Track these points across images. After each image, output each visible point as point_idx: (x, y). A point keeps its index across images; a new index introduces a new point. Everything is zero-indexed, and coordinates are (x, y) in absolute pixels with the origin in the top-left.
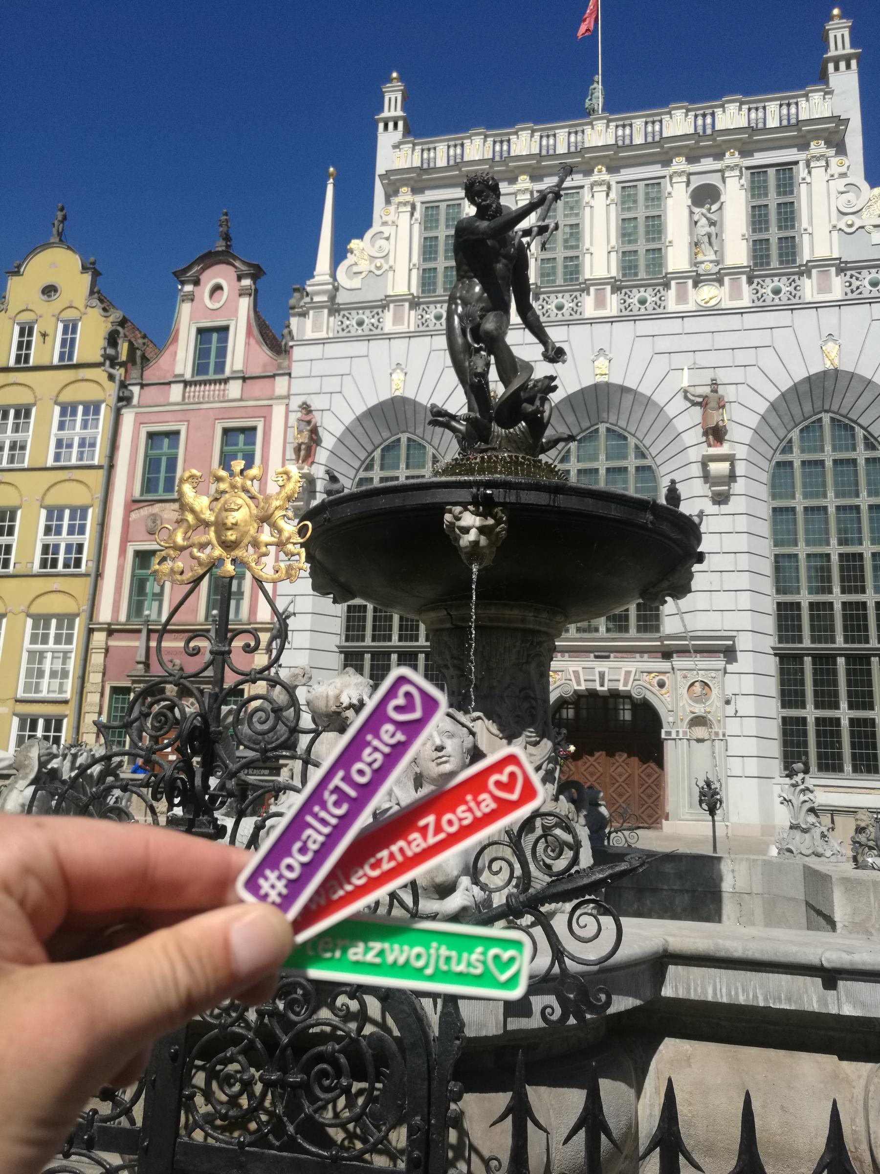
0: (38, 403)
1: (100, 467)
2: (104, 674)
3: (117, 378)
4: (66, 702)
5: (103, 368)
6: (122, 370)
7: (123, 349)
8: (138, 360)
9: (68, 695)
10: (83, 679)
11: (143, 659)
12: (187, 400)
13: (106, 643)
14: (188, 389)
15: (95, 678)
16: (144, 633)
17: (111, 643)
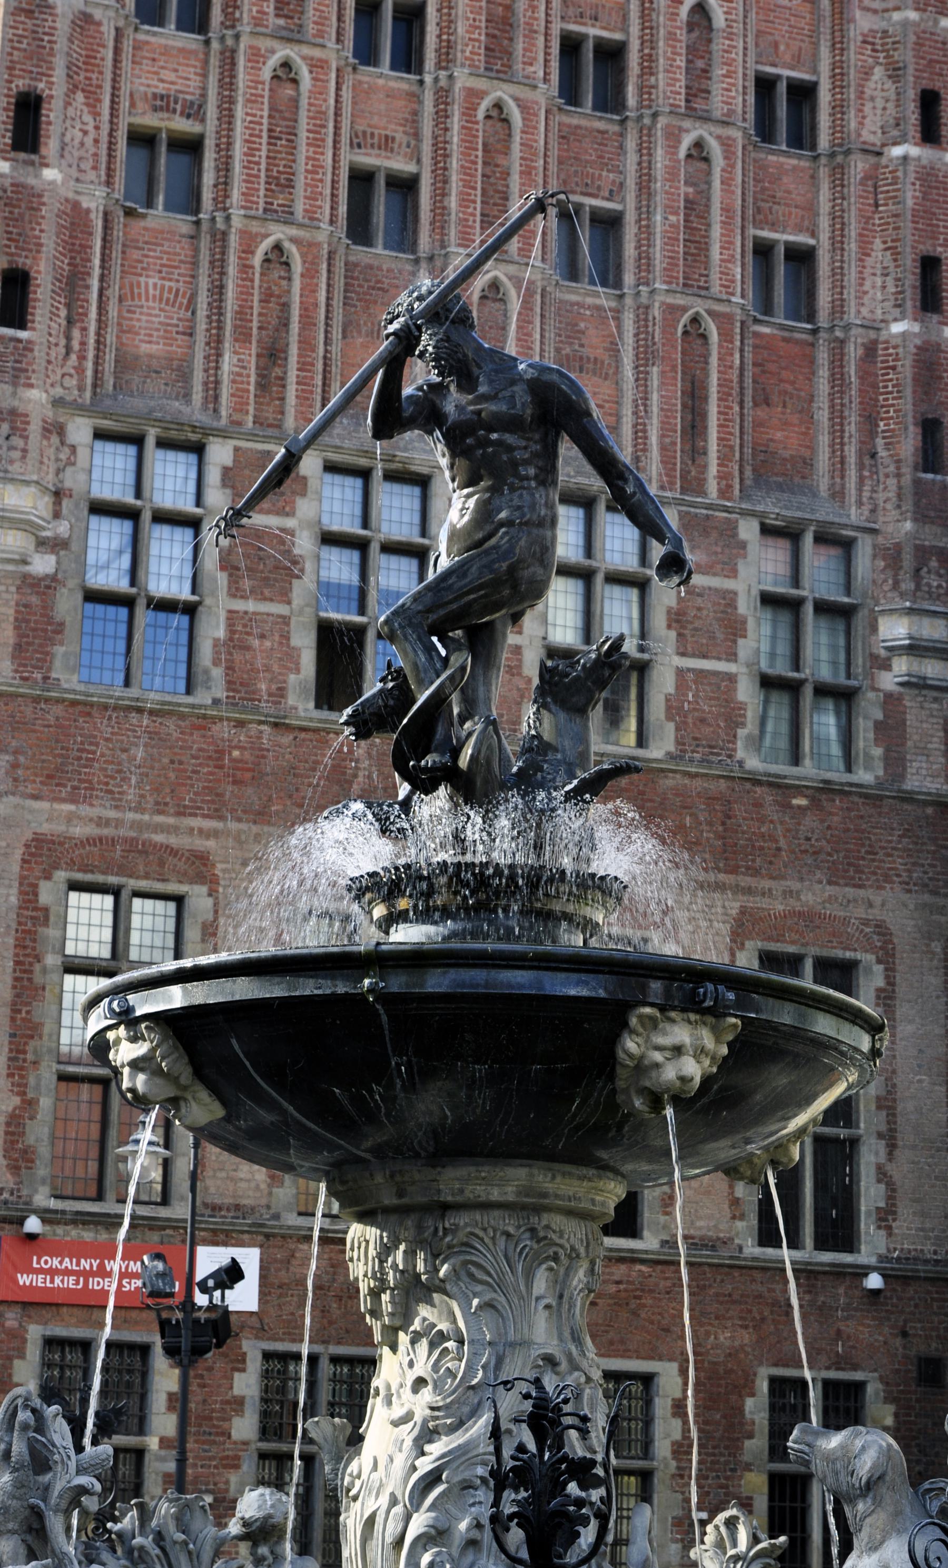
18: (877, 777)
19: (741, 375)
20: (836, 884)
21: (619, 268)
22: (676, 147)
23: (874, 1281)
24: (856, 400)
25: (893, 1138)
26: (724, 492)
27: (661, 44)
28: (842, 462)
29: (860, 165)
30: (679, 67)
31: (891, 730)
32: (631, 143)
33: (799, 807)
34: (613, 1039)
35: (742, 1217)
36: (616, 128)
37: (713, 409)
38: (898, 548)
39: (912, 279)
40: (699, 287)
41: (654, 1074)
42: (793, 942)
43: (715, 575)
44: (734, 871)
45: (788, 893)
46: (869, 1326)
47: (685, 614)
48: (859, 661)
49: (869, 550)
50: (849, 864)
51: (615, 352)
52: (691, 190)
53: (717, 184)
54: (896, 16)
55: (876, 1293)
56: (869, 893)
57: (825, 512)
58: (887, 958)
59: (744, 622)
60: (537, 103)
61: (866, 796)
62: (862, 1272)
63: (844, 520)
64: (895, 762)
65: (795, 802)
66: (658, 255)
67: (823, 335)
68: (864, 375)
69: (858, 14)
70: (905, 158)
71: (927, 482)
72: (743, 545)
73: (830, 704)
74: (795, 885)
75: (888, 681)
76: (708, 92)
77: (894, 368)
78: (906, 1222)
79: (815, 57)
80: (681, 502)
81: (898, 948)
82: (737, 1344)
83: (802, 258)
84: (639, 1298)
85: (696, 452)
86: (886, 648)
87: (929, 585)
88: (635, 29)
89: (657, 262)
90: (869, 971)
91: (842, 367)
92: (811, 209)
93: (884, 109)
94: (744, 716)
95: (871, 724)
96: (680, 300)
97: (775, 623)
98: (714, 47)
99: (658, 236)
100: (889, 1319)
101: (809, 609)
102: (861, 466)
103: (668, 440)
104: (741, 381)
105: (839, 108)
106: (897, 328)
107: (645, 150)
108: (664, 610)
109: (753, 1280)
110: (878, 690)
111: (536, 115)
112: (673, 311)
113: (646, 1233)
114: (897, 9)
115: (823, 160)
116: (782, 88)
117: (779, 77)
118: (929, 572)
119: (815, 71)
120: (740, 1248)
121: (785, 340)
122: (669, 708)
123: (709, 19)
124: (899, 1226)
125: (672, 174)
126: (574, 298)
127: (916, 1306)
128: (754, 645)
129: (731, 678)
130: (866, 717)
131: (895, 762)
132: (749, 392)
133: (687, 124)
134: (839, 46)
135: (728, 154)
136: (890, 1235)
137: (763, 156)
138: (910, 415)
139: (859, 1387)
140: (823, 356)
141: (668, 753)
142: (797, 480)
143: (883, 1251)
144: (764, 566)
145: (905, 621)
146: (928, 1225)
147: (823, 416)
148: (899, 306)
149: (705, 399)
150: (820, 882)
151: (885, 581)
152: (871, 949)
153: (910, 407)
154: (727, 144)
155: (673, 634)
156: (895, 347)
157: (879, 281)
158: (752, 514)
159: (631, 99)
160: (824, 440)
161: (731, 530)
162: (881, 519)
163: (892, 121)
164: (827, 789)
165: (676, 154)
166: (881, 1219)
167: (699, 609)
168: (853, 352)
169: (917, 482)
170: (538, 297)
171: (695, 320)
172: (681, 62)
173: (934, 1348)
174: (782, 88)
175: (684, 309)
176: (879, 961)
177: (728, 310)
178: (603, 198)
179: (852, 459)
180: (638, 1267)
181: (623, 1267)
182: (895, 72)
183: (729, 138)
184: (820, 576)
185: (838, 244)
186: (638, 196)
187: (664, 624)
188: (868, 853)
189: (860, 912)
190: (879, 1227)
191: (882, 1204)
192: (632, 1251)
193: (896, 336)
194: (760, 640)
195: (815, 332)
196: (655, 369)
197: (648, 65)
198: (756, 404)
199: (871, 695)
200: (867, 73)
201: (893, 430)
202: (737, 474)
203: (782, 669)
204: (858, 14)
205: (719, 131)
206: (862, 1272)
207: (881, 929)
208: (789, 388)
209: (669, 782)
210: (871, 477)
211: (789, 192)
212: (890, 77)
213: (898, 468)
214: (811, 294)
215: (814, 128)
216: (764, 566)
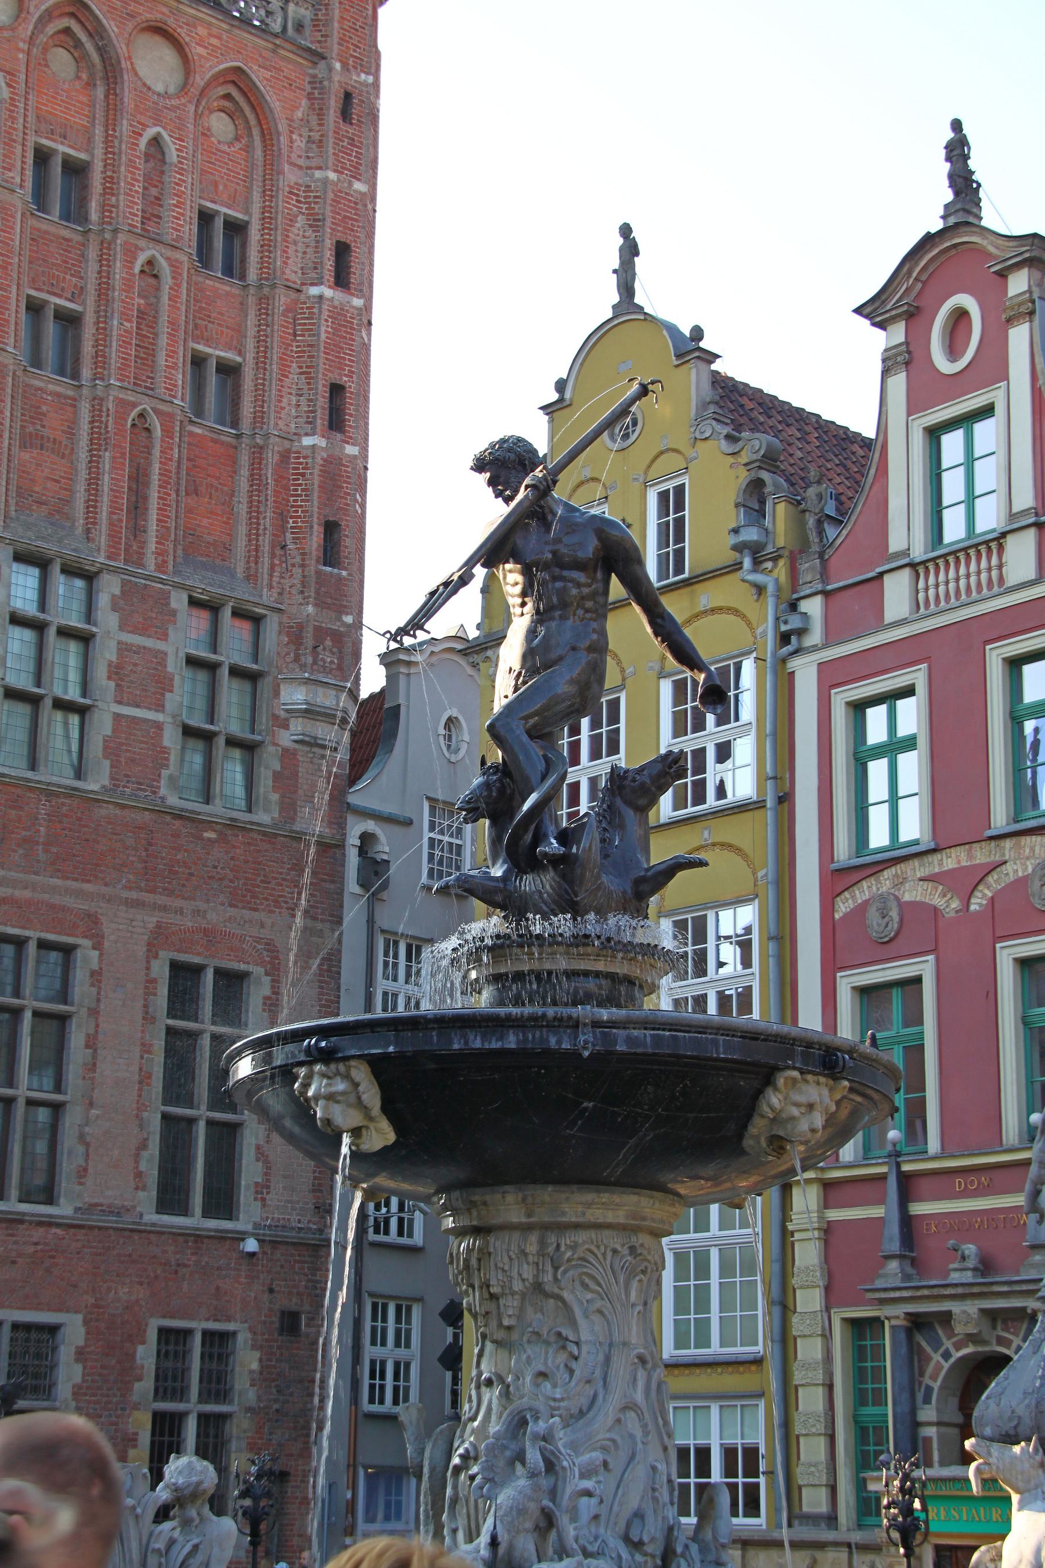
0: (628, 682)
1: (758, 805)
2: (828, 1289)
3: (771, 588)
4: (758, 1362)
5: (739, 575)
6: (781, 571)
7: (779, 515)
8: (813, 537)
9: (760, 1348)
10: (783, 1305)
11: (894, 1246)
12: (922, 610)
13: (821, 1218)
14: (921, 584)
15: (809, 1300)
16: (892, 1183)
17: (835, 1215)
18: (273, 819)
19: (179, 467)
20: (235, 906)
21: (77, 360)
22: (132, 263)
23: (251, 1245)
24: (271, 499)
26: (161, 567)
27: (123, 169)
28: (257, 550)
29: (283, 299)
30: (137, 192)
31: (287, 780)
32: (92, 253)
33: (209, 839)
34: (757, 1094)
35: (144, 1188)
36: (79, 238)
37: (154, 495)
38: (301, 627)
39: (322, 401)
40: (146, 387)
41: (789, 1126)
42: (199, 954)
43: (149, 636)
44: (152, 891)
45: (197, 912)
47: (122, 668)
48: (263, 719)
49: (276, 627)
51: (71, 433)
52: (142, 302)
53: (165, 299)
54: (318, 174)
55: (253, 1255)
56: (261, 916)
57: (242, 592)
59: (172, 680)
60: (14, 206)
61: (265, 834)
62: (240, 1237)
63: (256, 600)
64: (289, 808)
65: (206, 835)
66: (113, 356)
67: (245, 440)
68: (279, 478)
69: (286, 167)
70: (321, 297)
71: (325, 574)
72: (174, 613)
73: (237, 753)
74: (202, 905)
75: (286, 738)
76: (160, 218)
77: (303, 475)
79: (248, 199)
80: (125, 572)
82: (133, 1298)
83: (228, 371)
84: (53, 1257)
85: (137, 530)
86: (287, 711)
87: (323, 660)
88: (99, 151)
89: (113, 361)
91: (260, 469)
92: (239, 331)
93: (305, 253)
94: (167, 759)
95: (270, 774)
96: (131, 397)
97: (194, 680)
98: (166, 179)
99: (115, 338)
101: (225, 671)
102: (273, 555)
103: (115, 517)
104: (178, 473)
105: (266, 247)
106: (307, 441)
107: (105, 261)
108: (106, 664)
109: (150, 1243)
110: (277, 745)
111: (13, 217)
112: (125, 406)
113: (62, 1200)
114: (320, 168)
115: (252, 291)
116: (219, 224)
117: (217, 212)
118: (324, 649)
119: (247, 211)
120: (141, 1215)
121: (213, 440)
122: (106, 748)
123: (163, 154)
124: (272, 1198)
125: (128, 287)
126: (38, 383)
127: (282, 1266)
128: (178, 698)
129: (159, 726)
130: (267, 767)
131: (289, 808)
132: (183, 483)
133: (142, 243)
134: (269, 193)
135: (176, 275)
136: (264, 1206)
137: (201, 279)
138: (316, 515)
139: (232, 1335)
140: (244, 459)
141: (104, 787)
142: (218, 562)
144: (189, 632)
145: (303, 689)
146: (295, 1198)
147: (242, 509)
148: (310, 423)
149: (147, 484)
150: (223, 904)
151: (288, 654)
152: (262, 963)
153: (316, 509)
154: (174, 265)
155: (112, 684)
156: (305, 458)
157: (294, 399)
158: (182, 587)
159: (94, 216)
160: (242, 530)
161: (165, 597)
162: (287, 601)
163: (311, 265)
164: (233, 825)
165: (131, 268)
166: (257, 1192)
167: (136, 665)
168: (271, 458)
169: (318, 573)
170: (10, 379)
171: (141, 415)
172: (138, 188)
173: (293, 1304)
174: (219, 224)
175: (134, 405)
176: (267, 974)
177: (170, 410)
178: (67, 299)
179: (266, 549)
180: (54, 1230)
181: (42, 1230)
182: (316, 223)
183: (177, 261)
184: (235, 645)
185: (261, 364)
186: (98, 301)
187: (105, 675)
188: (262, 881)
190: (256, 1199)
192: (50, 1216)
193: (307, 447)
194: (184, 696)
195: (238, 436)
196: (107, 454)
197: (110, 187)
198: (187, 494)
199: (271, 749)
200: (293, 220)
201: (300, 528)
202: (171, 551)
203: (197, 721)
204: (286, 167)
205: (169, 253)
206: (240, 1237)
207: (271, 947)
208: (215, 483)
209: (104, 811)
210: (280, 565)
211: (221, 314)
212: (311, 226)
213: (303, 560)
214: (236, 403)
215: (243, 260)
216: (189, 632)
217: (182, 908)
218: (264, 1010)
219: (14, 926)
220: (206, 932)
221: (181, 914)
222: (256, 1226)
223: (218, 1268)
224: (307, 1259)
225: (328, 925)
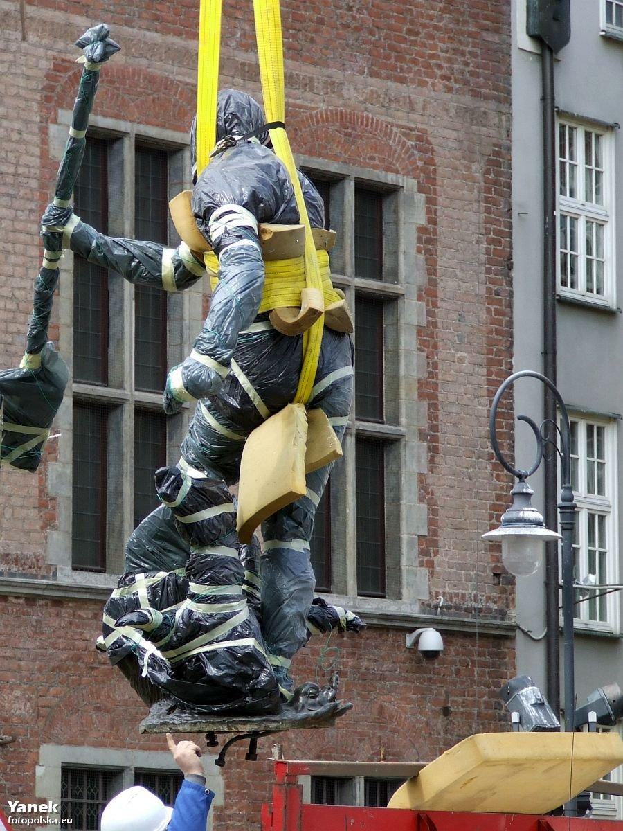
23: (431, 639)
25: (434, 439)
42: (335, 158)
46: (411, 701)
50: (392, 48)
55: (431, 655)
58: (428, 185)
74: (339, 76)
78: (446, 557)
81: (440, 170)
90: (410, 201)
100: (431, 692)
127: (458, 672)
136: (432, 574)
143: (426, 597)
150: (362, 73)
176: (421, 190)
188: (410, 32)
189: (400, 117)
191: (424, 532)
207: (423, 144)
217: (311, 79)
218: (419, 251)
219: (105, 115)
220: (345, 120)
221: (311, 90)
222: (426, 606)
223: (382, 678)
224: (488, 659)
225: (492, 105)
